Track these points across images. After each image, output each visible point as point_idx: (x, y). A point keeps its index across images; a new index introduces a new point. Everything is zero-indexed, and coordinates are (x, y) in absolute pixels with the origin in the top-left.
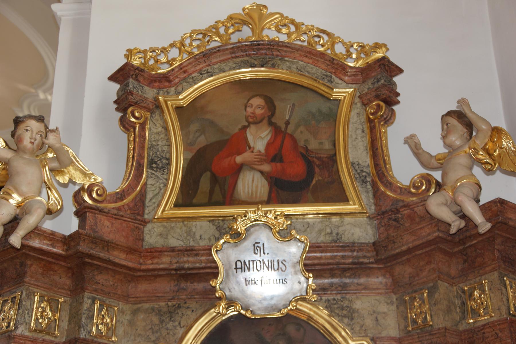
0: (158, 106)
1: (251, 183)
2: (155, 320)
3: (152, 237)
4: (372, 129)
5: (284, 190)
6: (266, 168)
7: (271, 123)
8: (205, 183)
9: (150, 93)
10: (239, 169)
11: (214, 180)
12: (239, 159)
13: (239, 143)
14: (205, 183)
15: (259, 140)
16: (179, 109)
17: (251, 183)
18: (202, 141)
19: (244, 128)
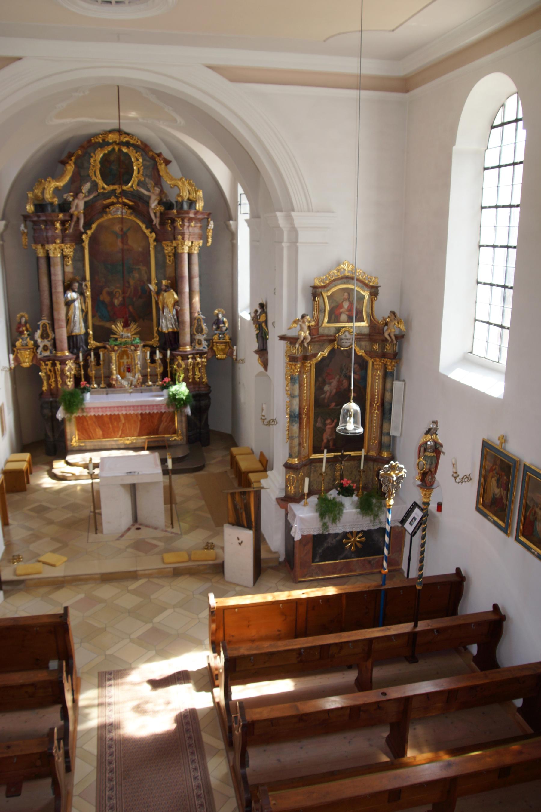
0: (322, 294)
1: (344, 317)
2: (319, 346)
3: (321, 330)
4: (372, 303)
5: (350, 320)
6: (347, 313)
7: (349, 301)
8: (333, 316)
9: (320, 290)
10: (341, 314)
11: (335, 316)
12: (341, 311)
13: (340, 306)
14: (333, 316)
15: (346, 305)
16: (328, 296)
17: (344, 317)
18: (333, 305)
19: (343, 302)
